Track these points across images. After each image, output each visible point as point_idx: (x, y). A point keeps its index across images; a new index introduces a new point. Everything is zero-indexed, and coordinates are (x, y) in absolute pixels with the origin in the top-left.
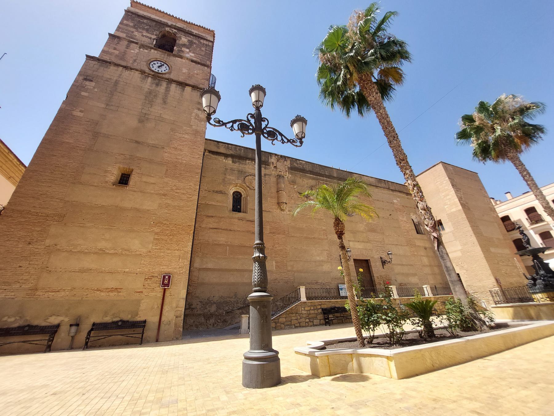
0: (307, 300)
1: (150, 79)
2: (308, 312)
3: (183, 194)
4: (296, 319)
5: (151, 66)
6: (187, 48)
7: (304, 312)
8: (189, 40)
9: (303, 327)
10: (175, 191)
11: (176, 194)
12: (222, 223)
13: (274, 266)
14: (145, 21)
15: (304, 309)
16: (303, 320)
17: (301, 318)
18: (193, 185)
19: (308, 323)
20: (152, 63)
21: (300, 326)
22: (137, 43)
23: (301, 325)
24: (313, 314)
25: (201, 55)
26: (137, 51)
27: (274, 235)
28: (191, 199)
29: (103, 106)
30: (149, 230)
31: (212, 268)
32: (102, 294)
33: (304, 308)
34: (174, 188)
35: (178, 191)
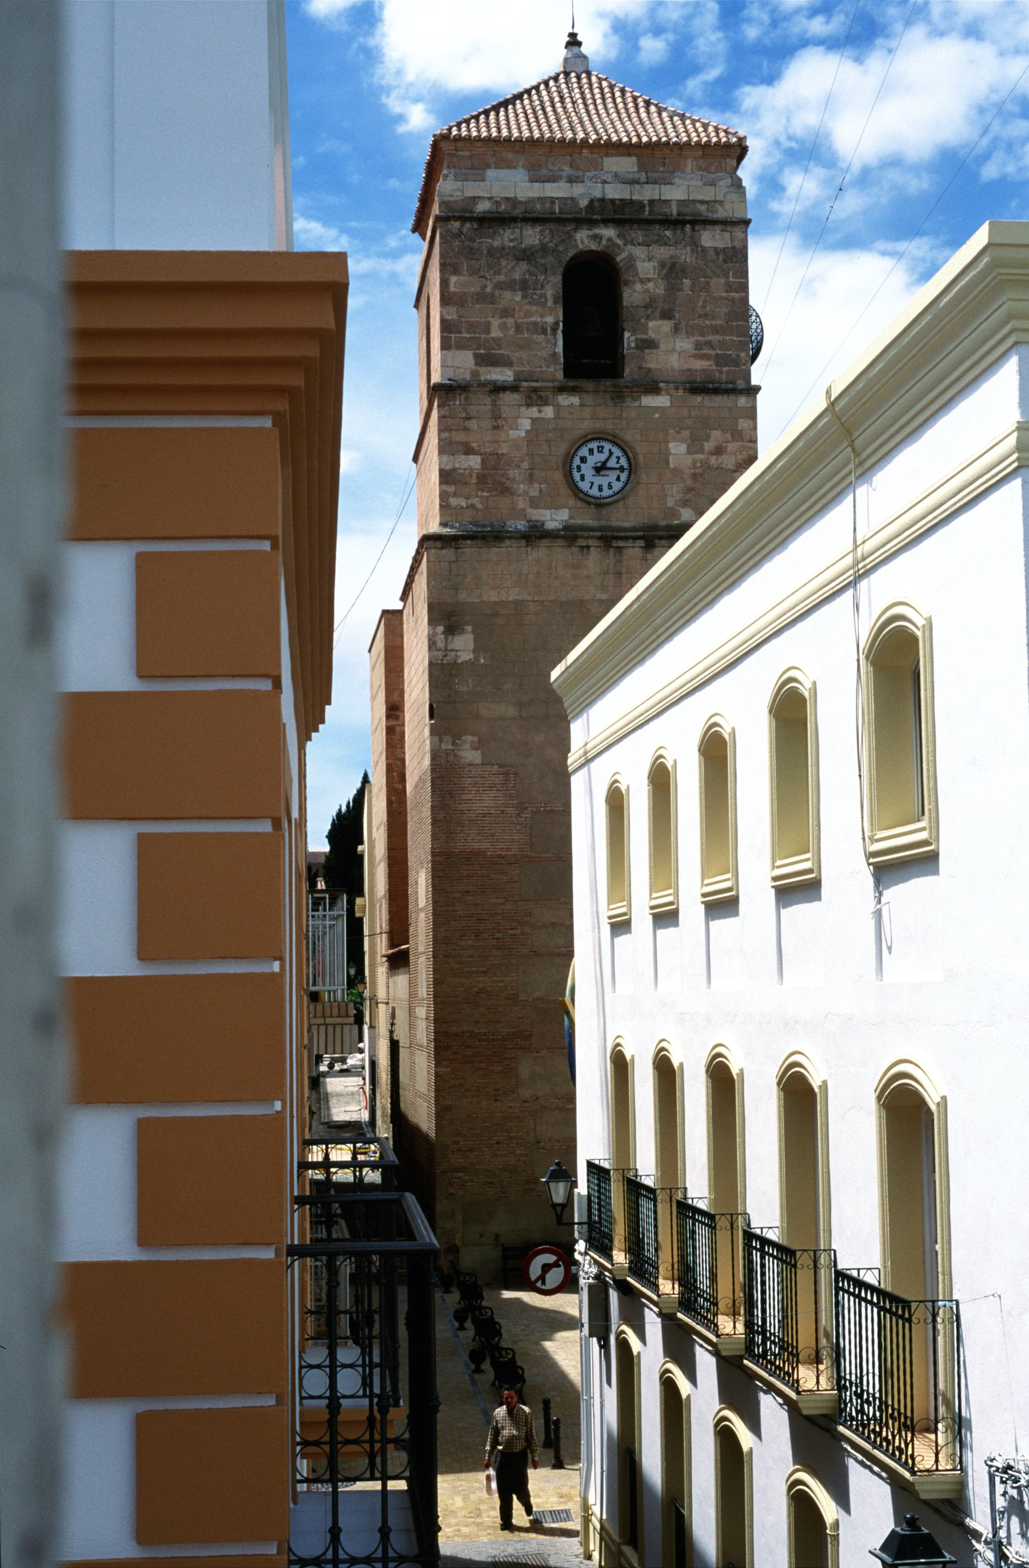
1: (594, 554)
5: (577, 476)
6: (666, 315)
8: (662, 265)
14: (506, 237)
20: (577, 461)
22: (514, 388)
25: (715, 330)
26: (526, 424)
29: (512, 712)
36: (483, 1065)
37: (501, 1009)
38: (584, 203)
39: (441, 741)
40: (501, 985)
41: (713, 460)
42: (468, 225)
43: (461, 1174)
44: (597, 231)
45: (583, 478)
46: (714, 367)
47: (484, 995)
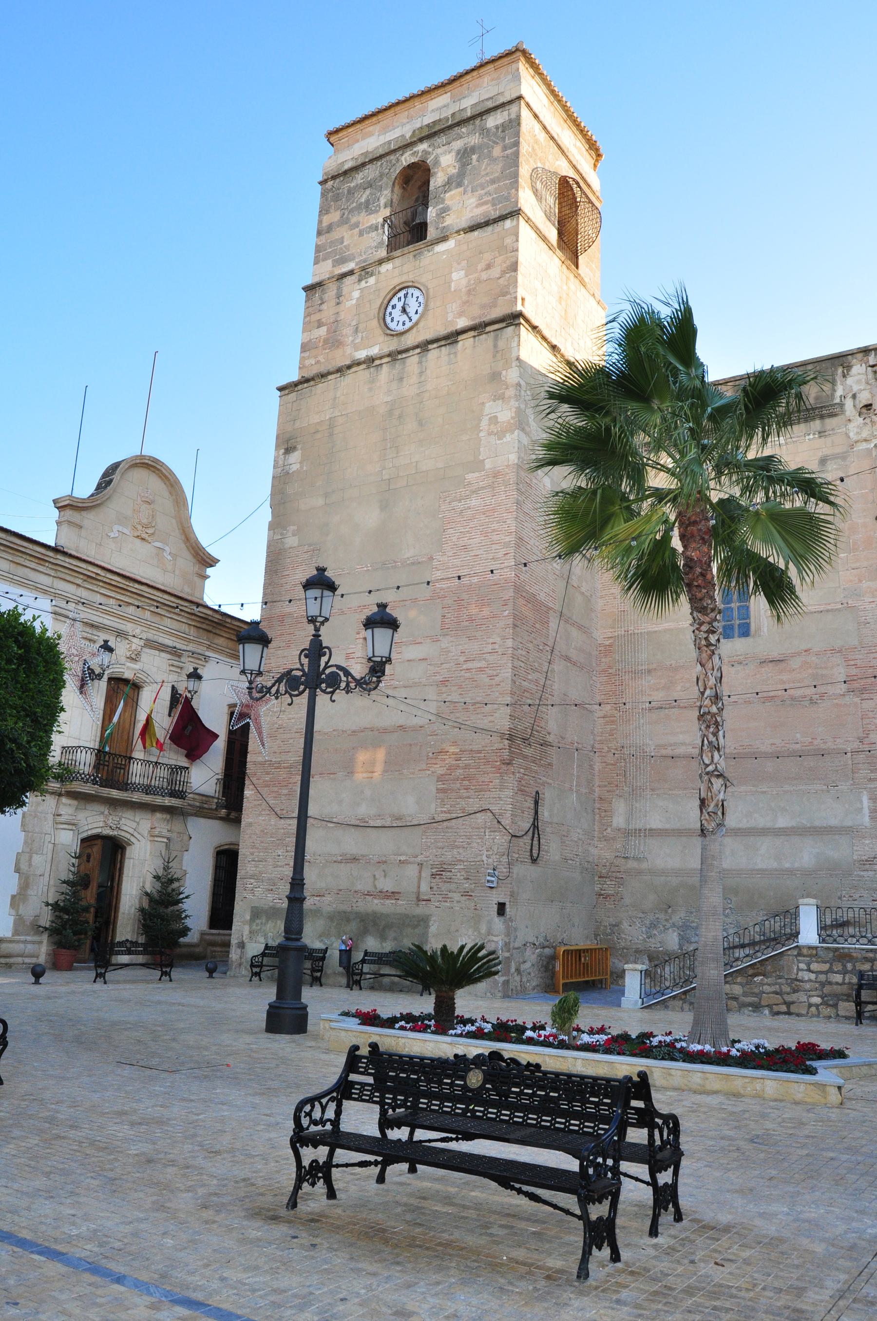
0: (824, 941)
2: (822, 978)
3: (481, 670)
4: (776, 993)
7: (806, 976)
9: (798, 1015)
10: (464, 667)
11: (468, 675)
12: (679, 688)
13: (866, 811)
14: (359, 178)
15: (805, 968)
16: (802, 997)
17: (795, 991)
18: (498, 640)
19: (818, 1009)
21: (789, 1013)
23: (792, 1011)
24: (837, 983)
25: (493, 182)
27: (865, 696)
28: (497, 678)
30: (428, 772)
31: (660, 827)
32: (376, 901)
33: (808, 965)
34: (462, 659)
35: (470, 665)
36: (276, 789)
37: (291, 741)
38: (408, 136)
39: (274, 533)
40: (293, 721)
41: (484, 275)
42: (338, 180)
43: (252, 881)
44: (415, 149)
45: (392, 320)
46: (491, 208)
47: (281, 731)
